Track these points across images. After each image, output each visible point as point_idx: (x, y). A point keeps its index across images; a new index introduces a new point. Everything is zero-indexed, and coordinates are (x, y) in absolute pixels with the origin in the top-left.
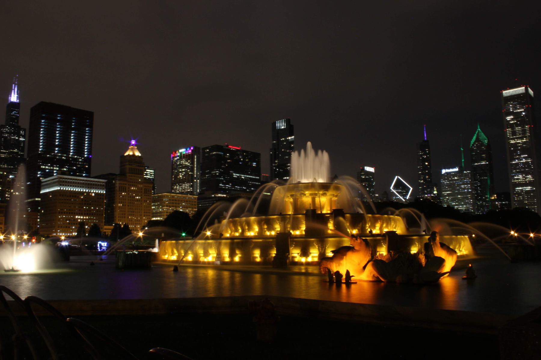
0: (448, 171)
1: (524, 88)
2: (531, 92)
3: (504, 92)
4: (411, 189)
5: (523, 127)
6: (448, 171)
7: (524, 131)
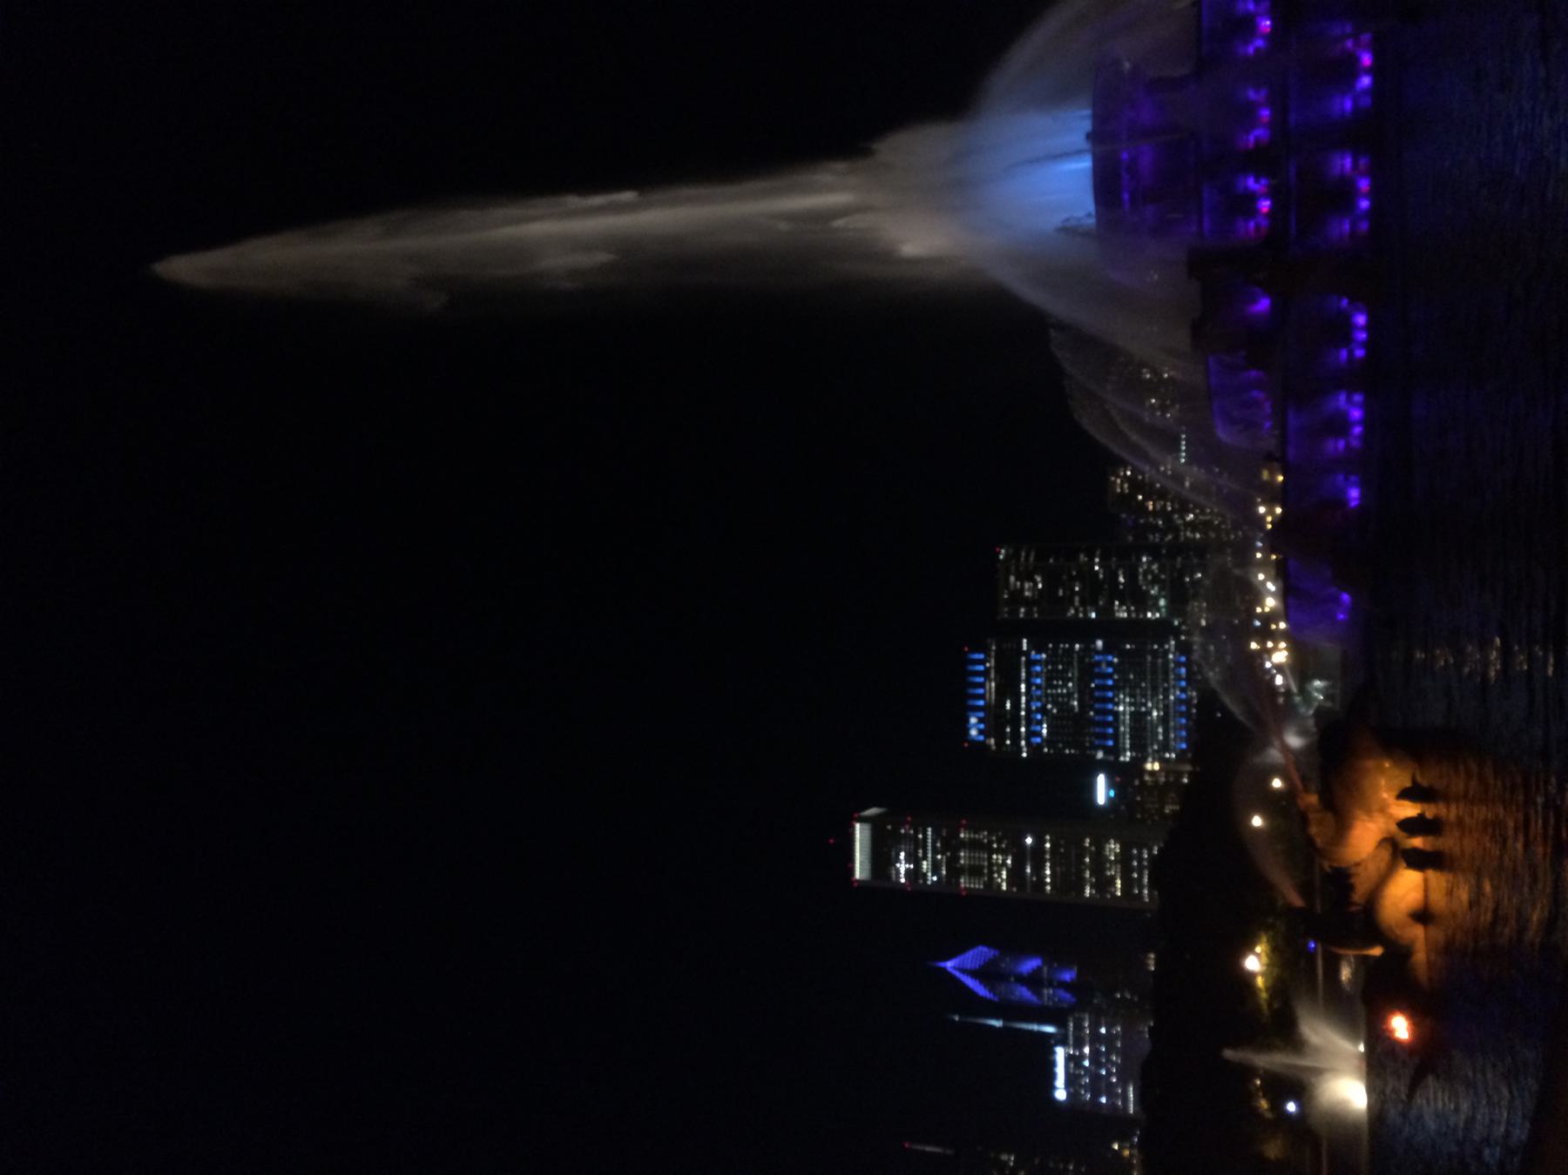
0: (1060, 1081)
1: (858, 826)
2: (872, 811)
3: (858, 875)
5: (963, 845)
6: (1060, 1081)
7: (974, 845)
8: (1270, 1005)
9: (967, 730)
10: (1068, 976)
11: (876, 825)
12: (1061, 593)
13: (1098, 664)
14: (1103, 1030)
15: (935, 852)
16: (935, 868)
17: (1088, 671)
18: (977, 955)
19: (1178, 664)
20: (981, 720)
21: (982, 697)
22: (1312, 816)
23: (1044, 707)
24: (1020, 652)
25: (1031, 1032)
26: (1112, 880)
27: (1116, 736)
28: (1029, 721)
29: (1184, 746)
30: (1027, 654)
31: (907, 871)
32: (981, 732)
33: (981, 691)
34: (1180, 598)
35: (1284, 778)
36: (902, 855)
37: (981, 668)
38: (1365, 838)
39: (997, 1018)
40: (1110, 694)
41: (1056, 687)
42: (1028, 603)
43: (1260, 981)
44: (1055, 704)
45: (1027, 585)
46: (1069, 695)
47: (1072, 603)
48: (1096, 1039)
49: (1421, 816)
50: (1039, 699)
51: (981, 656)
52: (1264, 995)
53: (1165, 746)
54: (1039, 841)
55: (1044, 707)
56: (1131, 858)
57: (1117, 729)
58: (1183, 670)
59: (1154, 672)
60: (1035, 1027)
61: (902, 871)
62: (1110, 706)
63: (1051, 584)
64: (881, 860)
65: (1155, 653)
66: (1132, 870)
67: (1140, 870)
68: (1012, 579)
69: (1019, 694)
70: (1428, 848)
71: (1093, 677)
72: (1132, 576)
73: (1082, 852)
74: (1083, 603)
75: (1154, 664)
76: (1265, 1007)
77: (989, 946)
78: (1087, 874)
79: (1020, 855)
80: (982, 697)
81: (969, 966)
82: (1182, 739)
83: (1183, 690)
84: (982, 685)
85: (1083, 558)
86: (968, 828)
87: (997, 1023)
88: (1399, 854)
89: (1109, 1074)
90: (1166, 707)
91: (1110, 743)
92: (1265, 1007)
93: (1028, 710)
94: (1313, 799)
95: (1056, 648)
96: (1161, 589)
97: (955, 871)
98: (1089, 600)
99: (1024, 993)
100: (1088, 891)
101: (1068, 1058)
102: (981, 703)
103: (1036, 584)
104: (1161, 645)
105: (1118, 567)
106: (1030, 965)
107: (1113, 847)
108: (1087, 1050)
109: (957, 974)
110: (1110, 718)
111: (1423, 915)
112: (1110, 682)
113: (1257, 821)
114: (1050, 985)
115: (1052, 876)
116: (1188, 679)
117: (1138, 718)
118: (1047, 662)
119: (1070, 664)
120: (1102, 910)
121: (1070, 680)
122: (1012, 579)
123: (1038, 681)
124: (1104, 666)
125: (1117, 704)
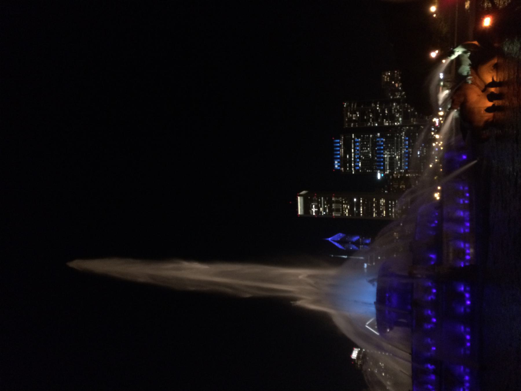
1: (299, 198)
3: (299, 213)
5: (333, 202)
7: (337, 202)
12: (365, 118)
13: (378, 141)
15: (324, 205)
16: (325, 210)
17: (375, 144)
19: (405, 140)
20: (339, 162)
21: (339, 154)
23: (360, 157)
24: (352, 139)
26: (382, 212)
27: (384, 166)
28: (355, 162)
29: (407, 168)
30: (354, 139)
31: (315, 211)
32: (339, 166)
33: (338, 152)
36: (314, 206)
37: (338, 145)
39: (345, 255)
40: (382, 151)
41: (364, 150)
42: (355, 121)
44: (363, 156)
45: (354, 115)
46: (368, 152)
47: (369, 121)
50: (358, 154)
51: (338, 141)
53: (401, 168)
55: (360, 157)
56: (389, 204)
57: (384, 163)
58: (407, 142)
59: (397, 143)
62: (382, 156)
63: (362, 114)
64: (307, 208)
65: (397, 137)
66: (389, 208)
67: (392, 208)
68: (349, 114)
69: (351, 153)
71: (376, 146)
72: (390, 111)
73: (373, 203)
74: (373, 121)
75: (397, 140)
78: (374, 210)
79: (352, 204)
80: (339, 154)
81: (336, 239)
82: (407, 166)
83: (407, 149)
84: (339, 150)
85: (373, 105)
86: (335, 197)
90: (401, 155)
93: (354, 158)
95: (364, 136)
97: (331, 210)
98: (375, 120)
100: (374, 215)
102: (339, 156)
103: (357, 115)
104: (400, 134)
105: (385, 108)
107: (383, 201)
110: (382, 160)
112: (382, 148)
114: (362, 244)
115: (363, 211)
116: (409, 145)
117: (392, 159)
118: (360, 142)
119: (369, 142)
121: (369, 147)
122: (349, 114)
123: (358, 148)
124: (380, 142)
125: (385, 155)
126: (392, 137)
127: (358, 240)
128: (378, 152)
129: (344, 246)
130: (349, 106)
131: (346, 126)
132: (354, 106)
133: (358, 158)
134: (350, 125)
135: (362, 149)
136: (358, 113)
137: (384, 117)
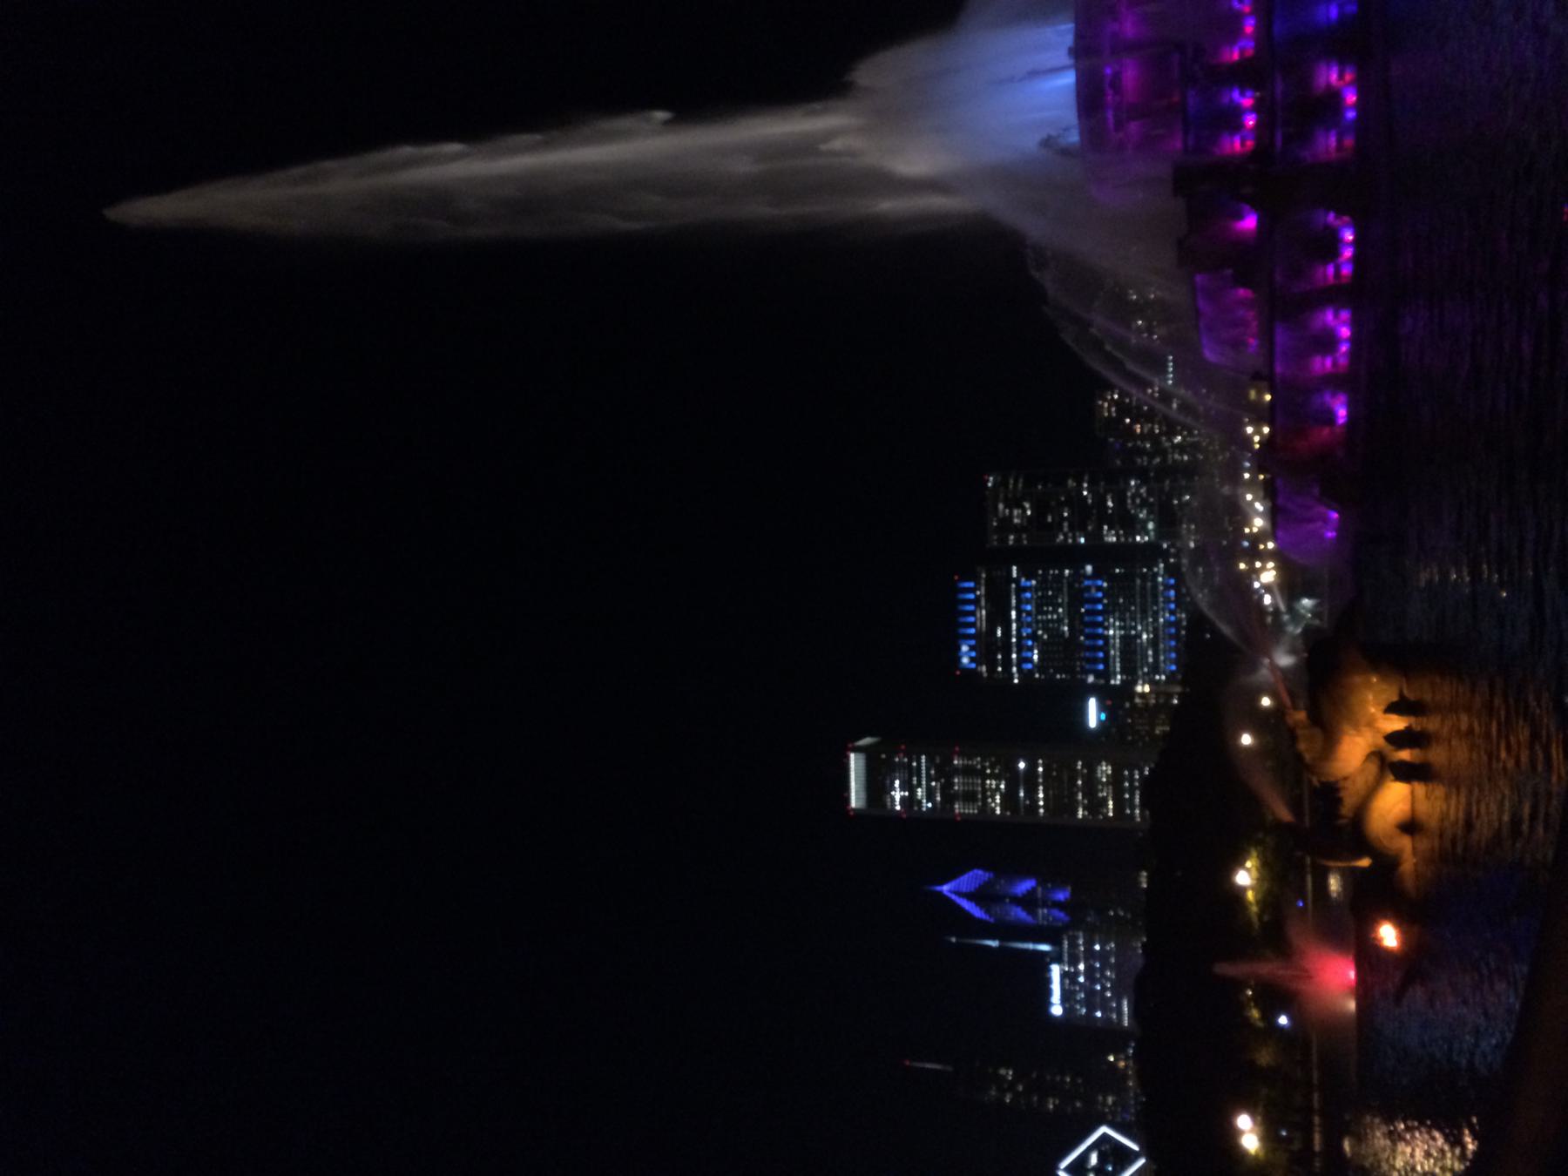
0: (1056, 997)
1: (852, 756)
3: (853, 804)
4: (1104, 1129)
6: (1056, 997)
7: (967, 771)
8: (1260, 916)
9: (959, 659)
10: (1061, 896)
11: (871, 755)
12: (1050, 519)
13: (1088, 588)
14: (1097, 947)
15: (929, 779)
16: (930, 796)
17: (1078, 597)
18: (972, 879)
19: (1167, 587)
20: (972, 648)
21: (972, 625)
22: (1300, 732)
23: (1035, 633)
24: (1010, 580)
25: (1027, 951)
26: (1105, 800)
27: (1106, 661)
29: (1174, 668)
30: (1017, 581)
31: (902, 798)
32: (972, 660)
33: (972, 619)
34: (1169, 521)
35: (1274, 695)
36: (897, 783)
37: (972, 596)
38: (1353, 752)
39: (993, 938)
40: (1100, 619)
41: (1047, 613)
42: (1018, 530)
43: (1250, 895)
44: (1045, 630)
45: (1016, 512)
46: (1060, 621)
47: (1060, 528)
48: (1090, 955)
49: (1408, 729)
50: (1029, 625)
51: (972, 585)
52: (1254, 909)
53: (1155, 669)
54: (1032, 767)
55: (1035, 633)
56: (1123, 779)
58: (1172, 593)
59: (1143, 596)
60: (1031, 946)
61: (898, 798)
62: (1100, 631)
64: (876, 788)
65: (1144, 577)
66: (1123, 791)
67: (1132, 791)
70: (1417, 761)
72: (1120, 500)
74: (1071, 528)
75: (1143, 588)
76: (1255, 919)
77: (985, 869)
78: (1080, 797)
80: (972, 625)
83: (1172, 613)
84: (972, 613)
85: (1071, 483)
86: (961, 755)
87: (994, 944)
88: (1386, 767)
89: (1104, 989)
90: (1155, 631)
91: (1101, 667)
92: (1255, 919)
93: (1019, 636)
94: (1301, 715)
95: (1045, 575)
96: (1149, 513)
97: (949, 797)
98: (1078, 526)
99: (1019, 914)
100: (1080, 813)
101: (1064, 975)
102: (972, 631)
103: (1024, 510)
104: (1150, 569)
105: (1106, 493)
106: (1025, 886)
107: (1105, 770)
108: (1081, 967)
109: (953, 897)
110: (1101, 642)
111: (1410, 826)
112: (1100, 607)
113: (1246, 740)
114: (1045, 905)
115: (1045, 799)
116: (1178, 602)
117: (1128, 642)
118: (1036, 589)
120: (1098, 833)
121: (1060, 605)
122: (1001, 506)
123: (1029, 608)
125: (1107, 628)
126: (1128, 577)
127: (1034, 889)
128: (1087, 619)
129: (988, 912)
130: (1002, 484)
131: (994, 540)
132: (1016, 484)
133: (1029, 637)
134: (1004, 540)
135: (1039, 611)
136: (1027, 505)
137: (1103, 517)
